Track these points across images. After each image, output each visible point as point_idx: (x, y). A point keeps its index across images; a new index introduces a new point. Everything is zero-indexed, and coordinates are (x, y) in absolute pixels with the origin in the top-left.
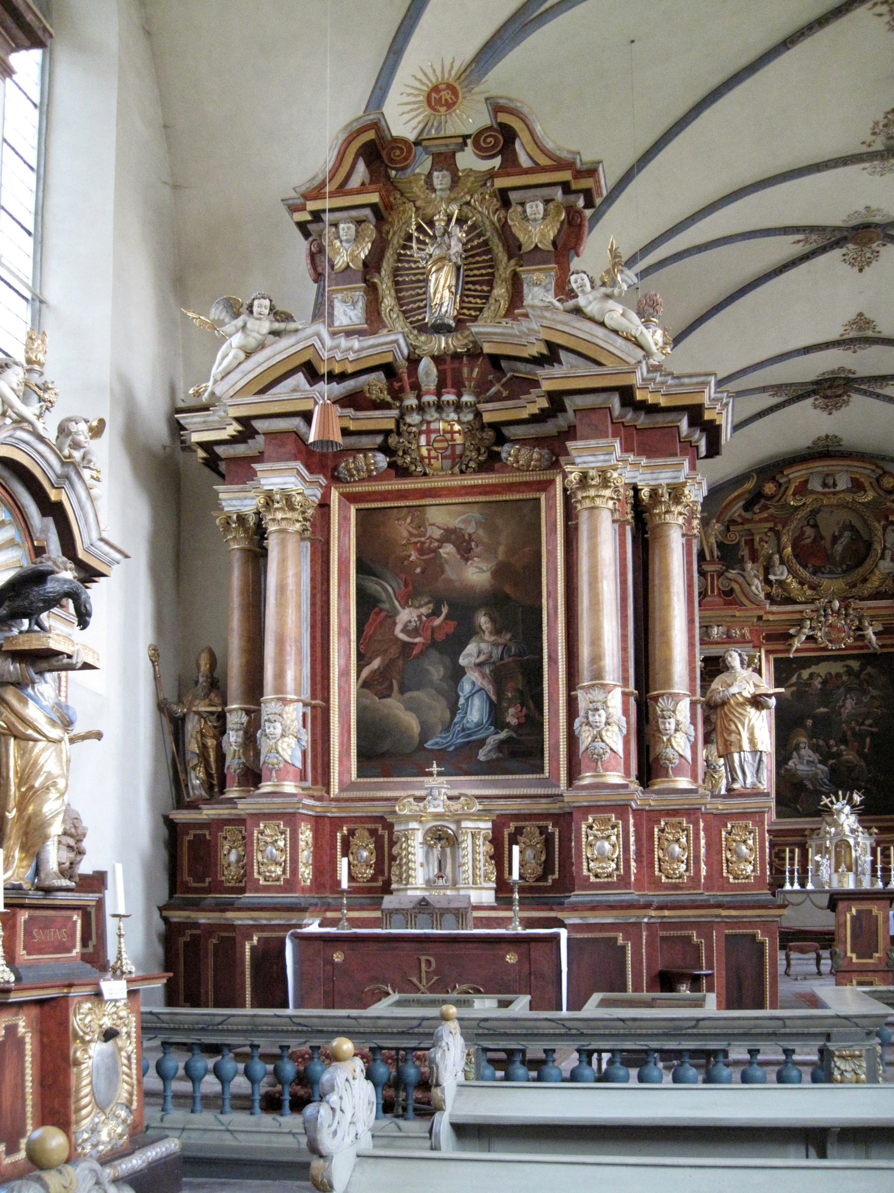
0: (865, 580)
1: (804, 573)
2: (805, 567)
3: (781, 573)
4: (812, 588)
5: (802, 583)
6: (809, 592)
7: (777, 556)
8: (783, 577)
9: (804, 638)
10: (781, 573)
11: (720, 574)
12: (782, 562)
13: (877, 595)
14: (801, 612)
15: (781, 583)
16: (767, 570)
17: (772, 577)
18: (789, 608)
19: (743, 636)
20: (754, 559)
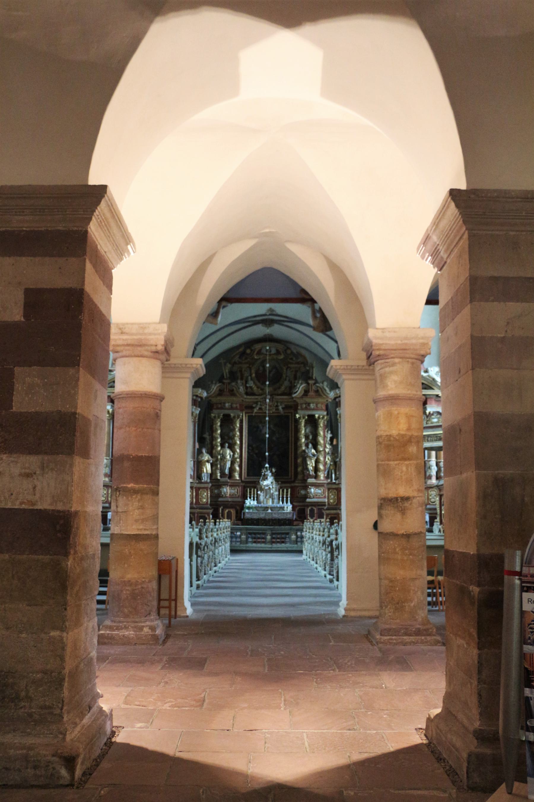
0: (279, 388)
1: (258, 384)
2: (259, 381)
3: (251, 384)
4: (262, 389)
5: (258, 387)
6: (261, 392)
7: (249, 377)
8: (252, 385)
9: (258, 408)
10: (251, 384)
11: (229, 383)
12: (252, 379)
13: (283, 394)
14: (257, 399)
15: (251, 387)
16: (246, 382)
17: (248, 385)
18: (253, 397)
19: (237, 407)
20: (242, 379)
